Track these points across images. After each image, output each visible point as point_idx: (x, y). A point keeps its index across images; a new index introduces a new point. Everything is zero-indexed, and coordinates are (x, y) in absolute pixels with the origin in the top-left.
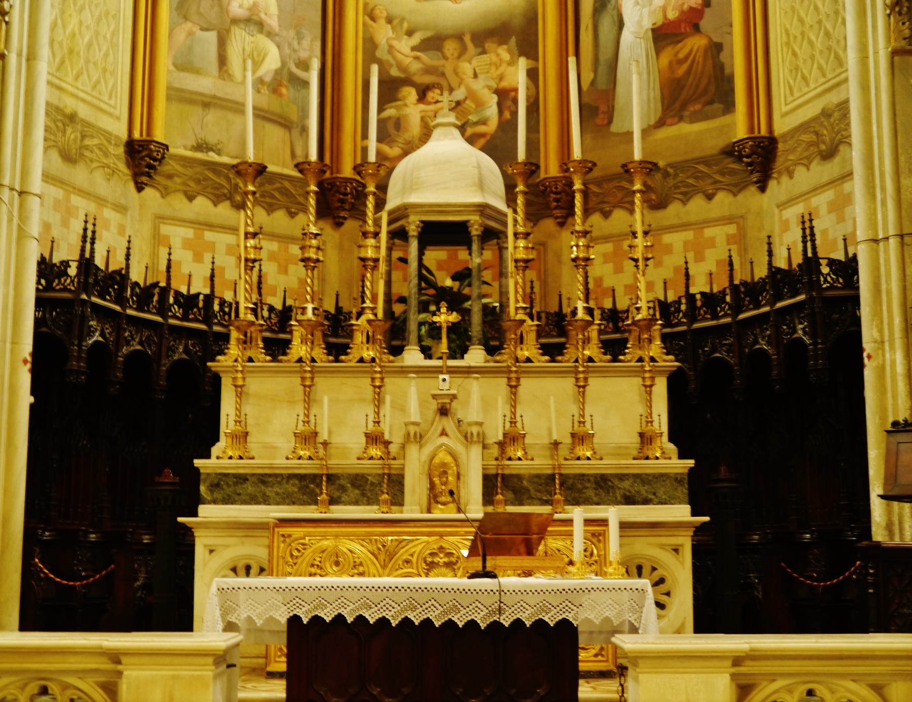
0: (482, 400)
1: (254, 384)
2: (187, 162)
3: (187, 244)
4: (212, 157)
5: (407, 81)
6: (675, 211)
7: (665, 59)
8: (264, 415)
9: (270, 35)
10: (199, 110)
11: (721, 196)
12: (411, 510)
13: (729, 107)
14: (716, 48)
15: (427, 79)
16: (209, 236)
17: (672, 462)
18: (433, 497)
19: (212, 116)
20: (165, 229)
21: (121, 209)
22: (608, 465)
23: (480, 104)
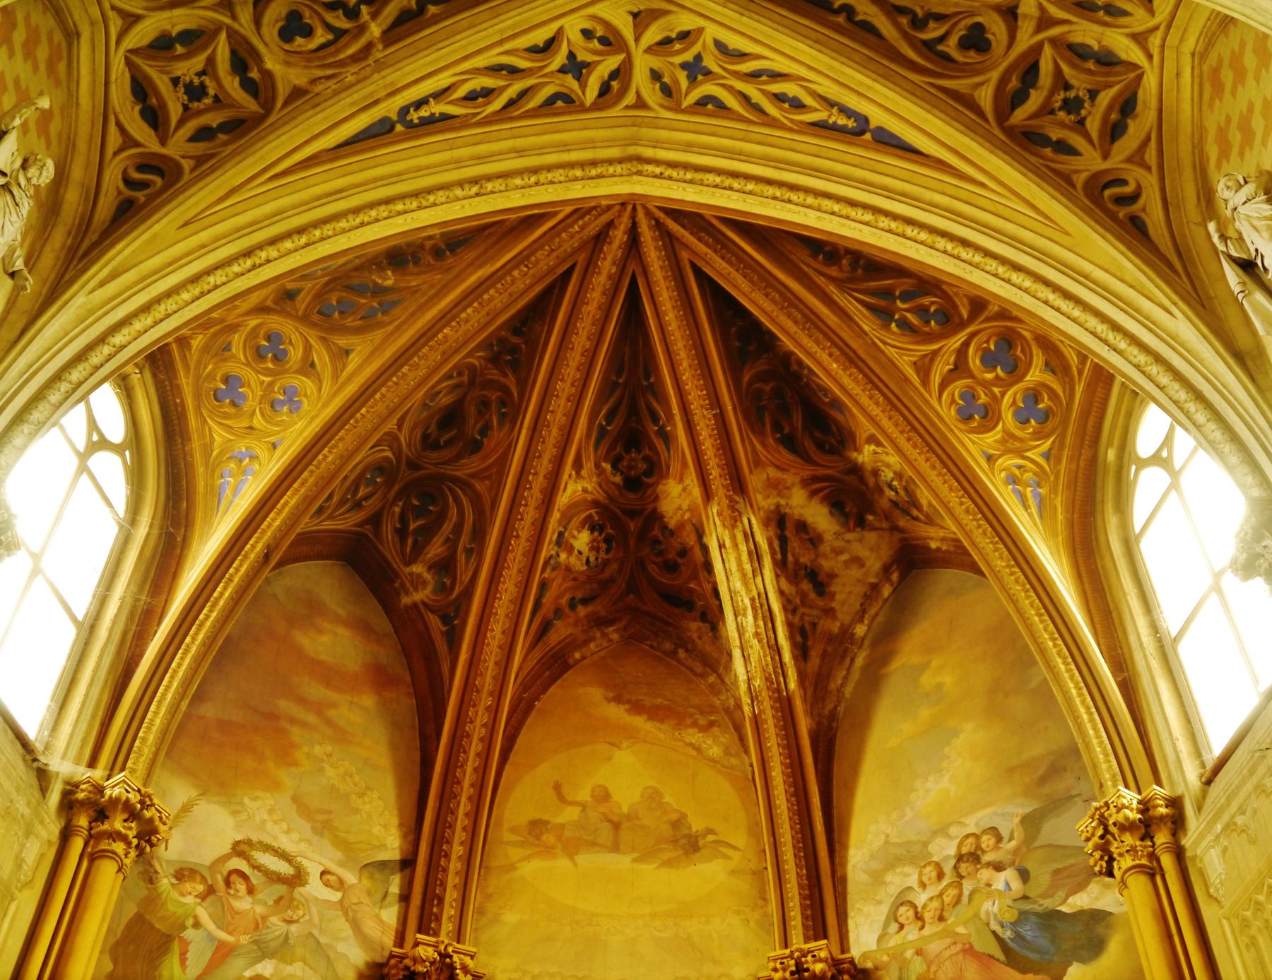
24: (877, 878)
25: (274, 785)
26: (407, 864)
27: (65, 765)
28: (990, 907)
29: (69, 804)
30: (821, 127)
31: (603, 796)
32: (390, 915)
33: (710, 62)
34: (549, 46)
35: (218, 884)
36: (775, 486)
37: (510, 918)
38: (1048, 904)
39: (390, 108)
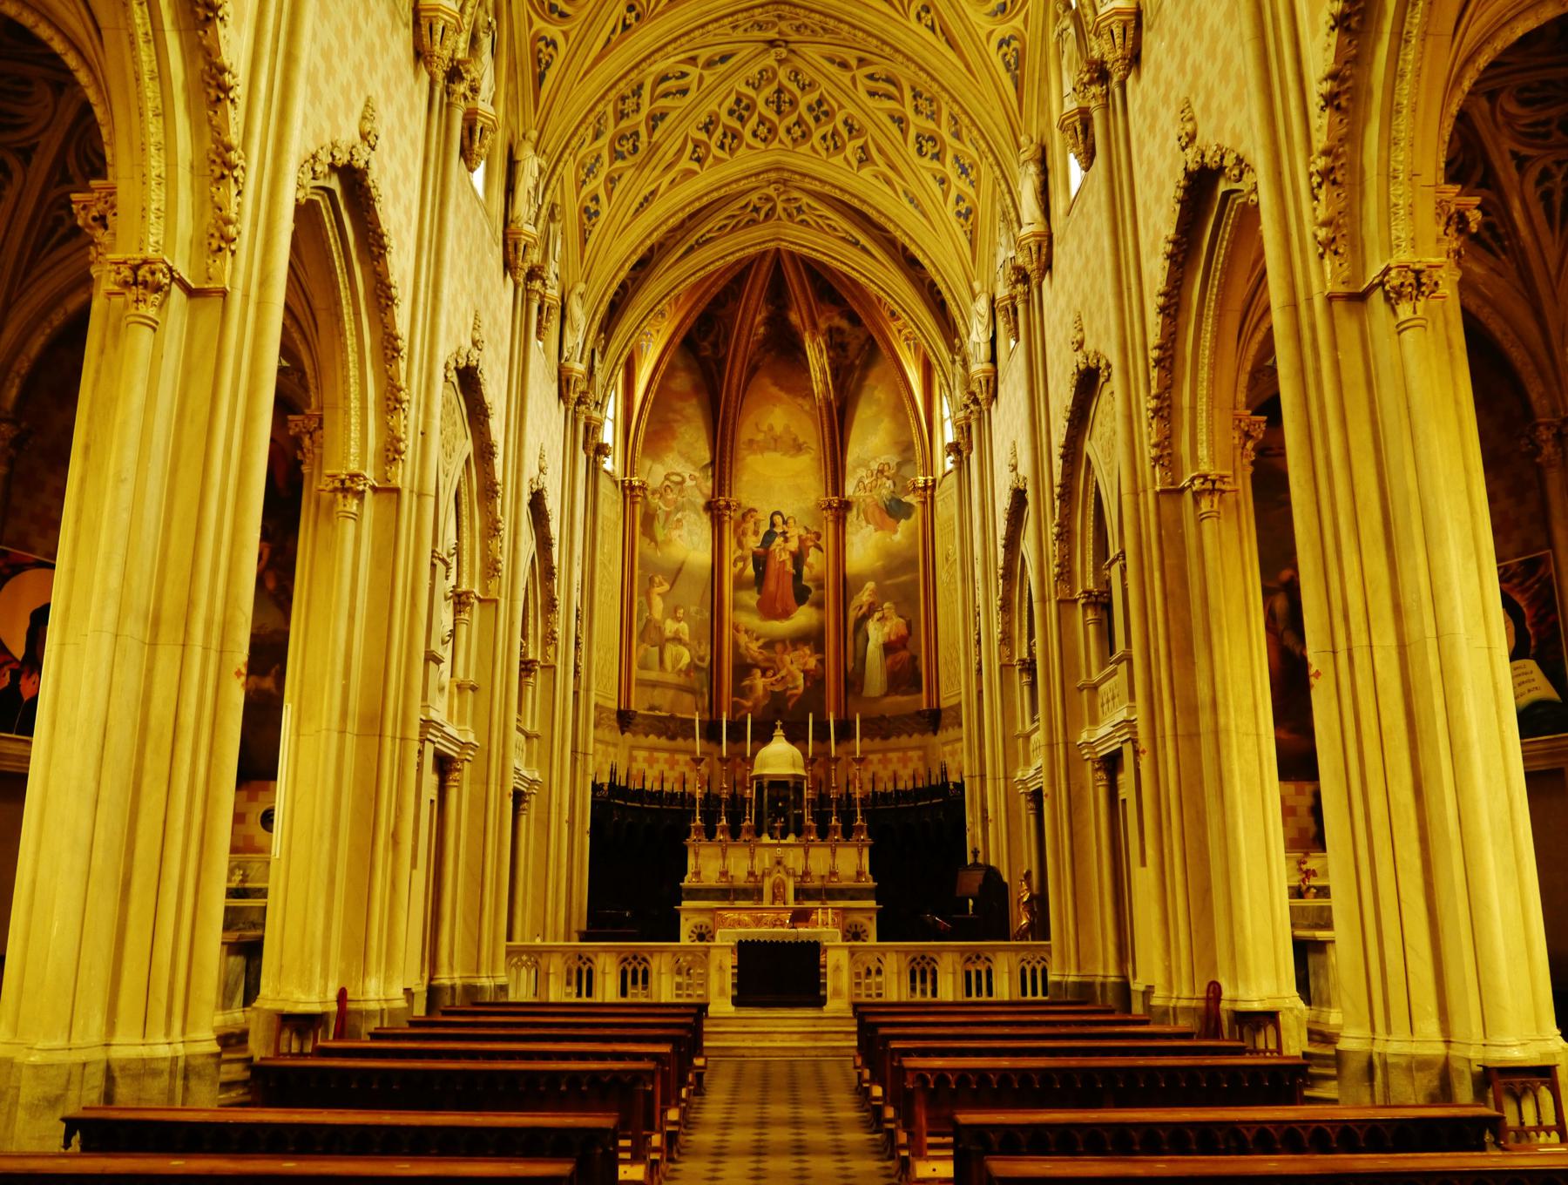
0: (794, 859)
1: (703, 851)
2: (645, 717)
3: (645, 760)
4: (658, 713)
5: (756, 666)
6: (893, 741)
7: (889, 661)
8: (706, 864)
9: (685, 645)
10: (649, 690)
11: (915, 736)
12: (766, 904)
13: (920, 691)
14: (914, 658)
15: (767, 664)
16: (656, 754)
17: (869, 882)
18: (775, 897)
19: (657, 692)
20: (635, 753)
21: (615, 745)
22: (845, 884)
23: (795, 679)
24: (855, 468)
25: (672, 449)
26: (713, 463)
27: (619, 478)
28: (884, 492)
29: (624, 488)
30: (843, 239)
31: (771, 428)
32: (710, 484)
33: (805, 208)
34: (747, 205)
35: (662, 492)
36: (829, 319)
37: (745, 478)
38: (899, 496)
39: (692, 242)
